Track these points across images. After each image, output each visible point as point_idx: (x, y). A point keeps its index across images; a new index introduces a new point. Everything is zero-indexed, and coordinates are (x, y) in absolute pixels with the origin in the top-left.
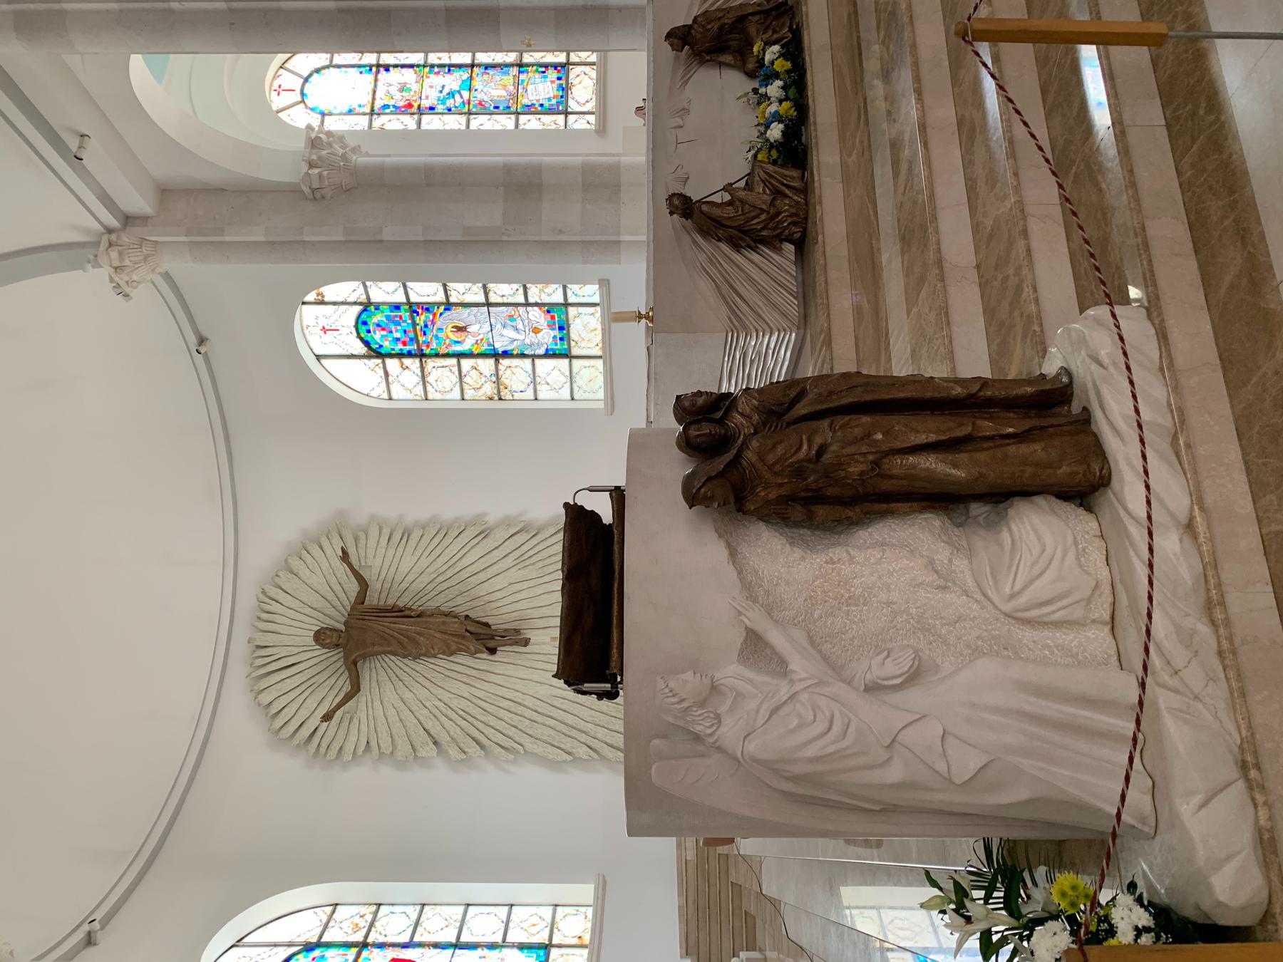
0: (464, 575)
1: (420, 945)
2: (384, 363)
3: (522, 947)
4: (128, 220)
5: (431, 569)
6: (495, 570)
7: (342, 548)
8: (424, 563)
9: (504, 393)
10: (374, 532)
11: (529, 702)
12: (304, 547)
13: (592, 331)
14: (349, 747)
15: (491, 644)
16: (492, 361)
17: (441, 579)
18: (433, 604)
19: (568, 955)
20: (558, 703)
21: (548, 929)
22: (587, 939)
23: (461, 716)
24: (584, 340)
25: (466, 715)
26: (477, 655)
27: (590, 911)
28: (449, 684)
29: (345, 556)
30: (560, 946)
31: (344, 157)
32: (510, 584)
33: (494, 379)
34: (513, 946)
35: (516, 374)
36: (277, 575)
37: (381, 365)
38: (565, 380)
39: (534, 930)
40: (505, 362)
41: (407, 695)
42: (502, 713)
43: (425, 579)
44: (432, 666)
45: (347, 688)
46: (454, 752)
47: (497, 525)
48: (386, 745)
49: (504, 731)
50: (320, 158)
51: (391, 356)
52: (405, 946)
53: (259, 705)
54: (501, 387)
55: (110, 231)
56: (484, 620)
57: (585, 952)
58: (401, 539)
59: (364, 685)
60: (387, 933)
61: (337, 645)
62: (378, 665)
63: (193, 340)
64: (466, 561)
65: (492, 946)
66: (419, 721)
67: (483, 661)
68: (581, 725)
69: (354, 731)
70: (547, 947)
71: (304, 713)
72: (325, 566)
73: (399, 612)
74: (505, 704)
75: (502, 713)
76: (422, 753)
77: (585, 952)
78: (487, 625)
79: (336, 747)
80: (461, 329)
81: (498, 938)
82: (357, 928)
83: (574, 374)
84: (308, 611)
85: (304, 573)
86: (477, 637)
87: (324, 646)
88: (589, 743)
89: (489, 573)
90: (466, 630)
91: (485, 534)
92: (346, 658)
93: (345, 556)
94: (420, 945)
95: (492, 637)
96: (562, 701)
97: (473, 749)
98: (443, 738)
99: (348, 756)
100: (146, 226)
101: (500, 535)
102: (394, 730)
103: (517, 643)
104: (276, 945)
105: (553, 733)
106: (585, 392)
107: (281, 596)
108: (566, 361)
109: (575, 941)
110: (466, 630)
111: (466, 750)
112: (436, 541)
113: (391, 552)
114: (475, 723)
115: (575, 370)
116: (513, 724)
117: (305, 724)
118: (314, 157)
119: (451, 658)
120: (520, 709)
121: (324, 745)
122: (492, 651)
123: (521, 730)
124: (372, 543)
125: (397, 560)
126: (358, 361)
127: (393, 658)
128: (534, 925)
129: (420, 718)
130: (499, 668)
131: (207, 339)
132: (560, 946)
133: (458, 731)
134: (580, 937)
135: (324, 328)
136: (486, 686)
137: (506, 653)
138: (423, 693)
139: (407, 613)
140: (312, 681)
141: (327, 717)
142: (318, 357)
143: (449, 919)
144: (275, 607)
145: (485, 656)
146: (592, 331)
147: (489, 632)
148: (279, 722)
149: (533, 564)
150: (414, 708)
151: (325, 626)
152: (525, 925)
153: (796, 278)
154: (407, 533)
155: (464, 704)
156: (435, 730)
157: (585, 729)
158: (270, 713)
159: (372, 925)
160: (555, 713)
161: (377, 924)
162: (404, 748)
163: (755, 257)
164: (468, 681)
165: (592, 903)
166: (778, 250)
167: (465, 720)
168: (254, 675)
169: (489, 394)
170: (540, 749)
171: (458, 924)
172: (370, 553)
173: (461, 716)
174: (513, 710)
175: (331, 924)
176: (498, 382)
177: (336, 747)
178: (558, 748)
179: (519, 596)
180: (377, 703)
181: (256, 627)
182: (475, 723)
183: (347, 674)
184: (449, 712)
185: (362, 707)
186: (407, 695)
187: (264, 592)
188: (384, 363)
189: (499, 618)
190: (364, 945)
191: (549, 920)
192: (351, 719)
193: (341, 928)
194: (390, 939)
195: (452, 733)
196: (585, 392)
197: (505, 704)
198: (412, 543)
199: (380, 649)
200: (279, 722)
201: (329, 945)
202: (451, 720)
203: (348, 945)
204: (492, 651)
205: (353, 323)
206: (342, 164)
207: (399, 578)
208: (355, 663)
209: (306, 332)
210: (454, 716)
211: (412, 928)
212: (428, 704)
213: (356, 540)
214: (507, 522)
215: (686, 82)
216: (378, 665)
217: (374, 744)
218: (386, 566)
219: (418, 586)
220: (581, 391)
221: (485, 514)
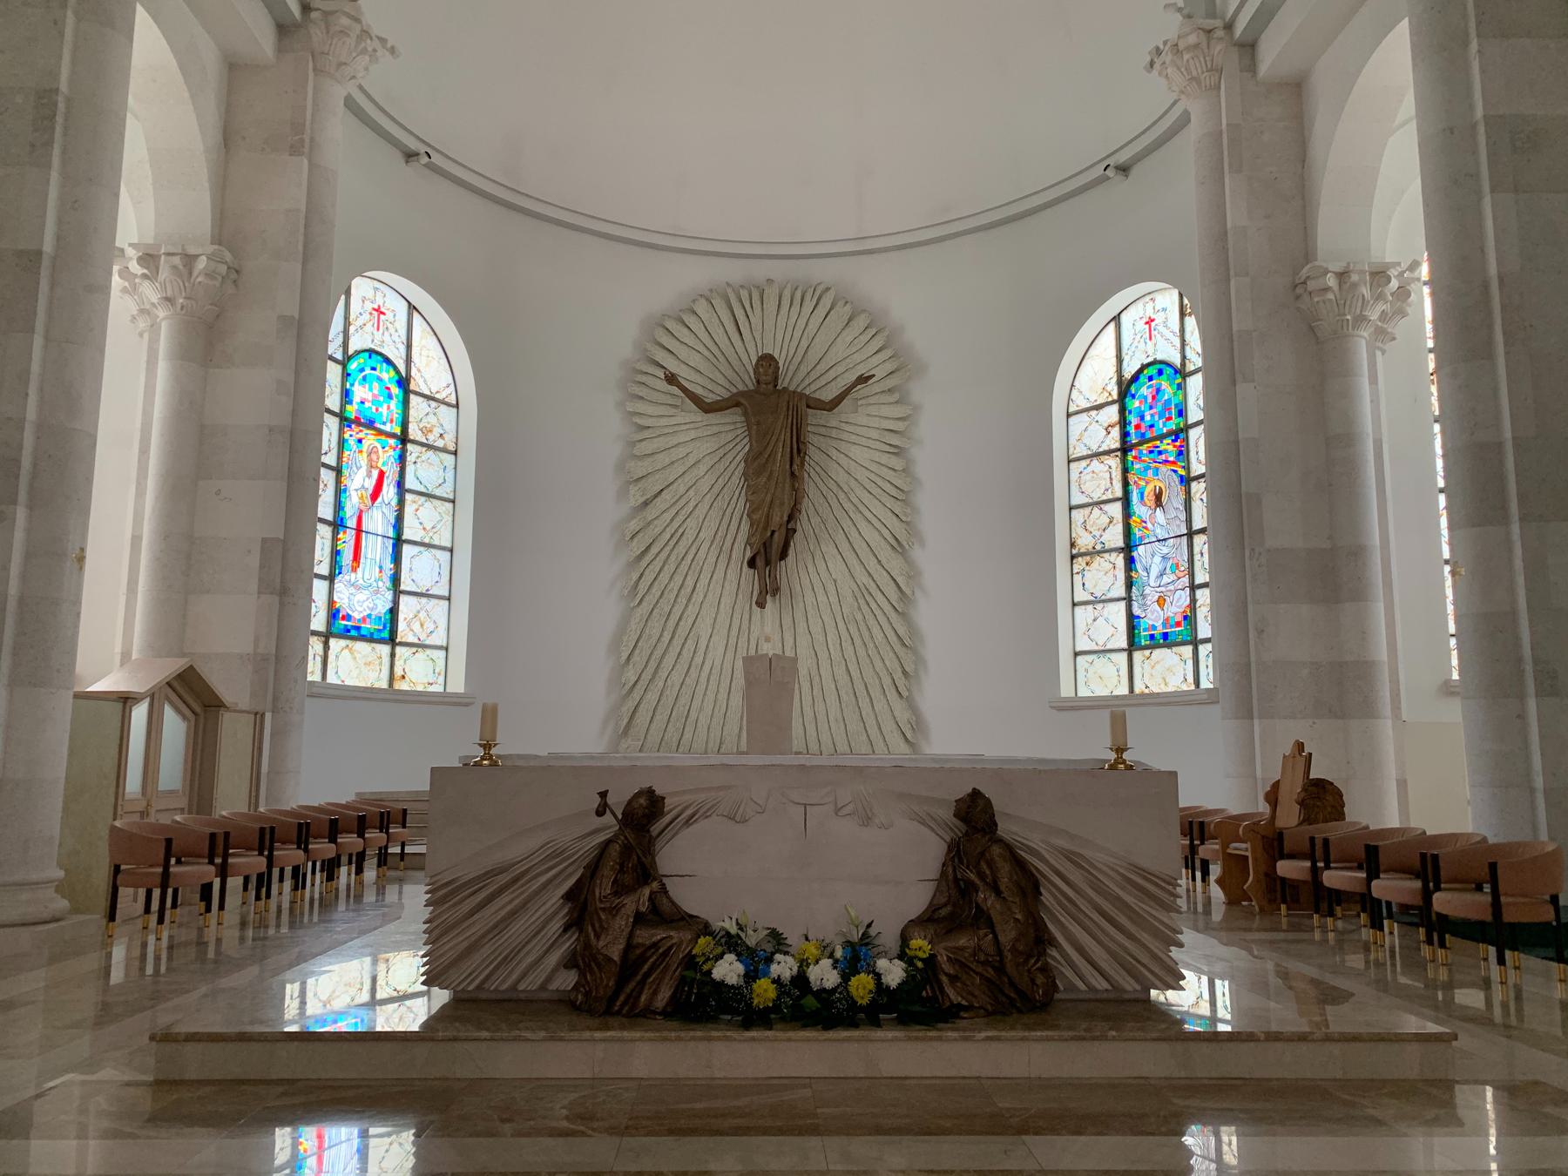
0: (846, 524)
1: (401, 503)
2: (1113, 402)
3: (394, 611)
4: (1249, 47)
5: (853, 483)
6: (852, 561)
7: (874, 376)
8: (861, 474)
9: (1081, 561)
11: (692, 610)
12: (878, 327)
13: (1164, 679)
14: (640, 407)
15: (760, 562)
16: (1121, 544)
17: (842, 496)
18: (810, 489)
19: (381, 664)
20: (690, 644)
21: (416, 641)
23: (676, 531)
24: (1153, 667)
26: (748, 547)
27: (438, 688)
30: (393, 655)
31: (1361, 319)
32: (835, 581)
33: (1098, 547)
34: (396, 602)
35: (1105, 576)
36: (847, 302)
37: (1110, 399)
38: (1101, 643)
39: (416, 626)
40: (1120, 560)
41: (703, 468)
42: (678, 579)
43: (841, 477)
44: (737, 493)
45: (710, 398)
46: (634, 525)
47: (908, 561)
49: (656, 583)
50: (1355, 286)
51: (1123, 411)
52: (400, 485)
53: (694, 301)
54: (1088, 558)
55: (1229, 27)
56: (791, 552)
57: (384, 685)
58: (890, 445)
59: (714, 418)
60: (418, 465)
61: (758, 382)
62: (739, 432)
63: (1122, 158)
64: (862, 525)
65: (396, 580)
66: (672, 483)
67: (741, 552)
68: (663, 674)
70: (392, 640)
71: (682, 352)
72: (858, 357)
73: (798, 449)
74: (690, 582)
75: (678, 579)
76: (633, 489)
77: (384, 685)
78: (783, 555)
79: (642, 392)
80: (1158, 497)
82: (426, 431)
83: (1108, 655)
84: (804, 344)
85: (848, 336)
86: (766, 545)
88: (641, 682)
89: (848, 554)
90: (773, 532)
91: (898, 547)
92: (742, 394)
93: (863, 379)
94: (401, 503)
95: (768, 563)
96: (693, 649)
97: (637, 547)
98: (651, 513)
100: (1241, 71)
101: (895, 564)
102: (660, 456)
103: (763, 593)
104: (409, 347)
105: (654, 640)
106: (1086, 671)
107: (821, 312)
108: (1124, 645)
109: (398, 671)
110: (773, 532)
111: (636, 540)
112: (888, 487)
113: (874, 434)
114: (668, 548)
115: (1113, 656)
116: (666, 592)
117: (671, 355)
118: (1355, 278)
119: (745, 516)
120: (683, 600)
121: (643, 378)
122: (752, 563)
123: (658, 602)
125: (864, 441)
126: (1115, 369)
127: (747, 448)
128: (422, 625)
129: (676, 484)
130: (732, 575)
131: (1127, 176)
132: (393, 655)
133: (658, 530)
134: (403, 677)
135: (1152, 320)
137: (751, 580)
138: (704, 486)
139: (797, 461)
140: (722, 359)
141: (671, 379)
142: (1117, 319)
143: (434, 530)
145: (749, 554)
146: (1164, 679)
147: (773, 561)
149: (860, 608)
150: (687, 478)
151: (781, 365)
152: (422, 615)
153: (514, 988)
154: (898, 452)
155: (690, 535)
156: (660, 504)
157: (657, 678)
158: (683, 314)
159: (429, 447)
160: (677, 642)
161: (431, 453)
162: (640, 468)
163: (556, 926)
164: (718, 537)
165: (448, 690)
166: (570, 962)
167: (672, 536)
168: (729, 291)
169: (1079, 542)
170: (634, 626)
171: (427, 540)
172: (873, 410)
173: (676, 531)
174: (682, 591)
175: (433, 404)
176: (1093, 553)
177: (642, 392)
178: (635, 646)
179: (820, 592)
180: (693, 434)
181: (796, 289)
182: (668, 548)
183: (726, 395)
184: (681, 518)
185: (692, 418)
186: (703, 468)
187: (828, 289)
188: (1113, 402)
189: (789, 569)
190: (404, 439)
191: (427, 642)
192: (676, 406)
193: (427, 414)
194: (410, 469)
195: (656, 522)
196: (1086, 671)
197: (690, 582)
198: (884, 459)
199: (754, 432)
200: (671, 325)
201: (406, 403)
202: (672, 520)
203: (405, 425)
204: (752, 563)
205: (1159, 357)
206: (1349, 317)
207: (843, 446)
208: (737, 405)
209: (1147, 298)
210: (676, 524)
211: (424, 490)
212: (691, 492)
214: (913, 574)
215: (923, 823)
216: (739, 432)
217: (646, 434)
218: (858, 430)
220: (1087, 665)
221: (922, 544)
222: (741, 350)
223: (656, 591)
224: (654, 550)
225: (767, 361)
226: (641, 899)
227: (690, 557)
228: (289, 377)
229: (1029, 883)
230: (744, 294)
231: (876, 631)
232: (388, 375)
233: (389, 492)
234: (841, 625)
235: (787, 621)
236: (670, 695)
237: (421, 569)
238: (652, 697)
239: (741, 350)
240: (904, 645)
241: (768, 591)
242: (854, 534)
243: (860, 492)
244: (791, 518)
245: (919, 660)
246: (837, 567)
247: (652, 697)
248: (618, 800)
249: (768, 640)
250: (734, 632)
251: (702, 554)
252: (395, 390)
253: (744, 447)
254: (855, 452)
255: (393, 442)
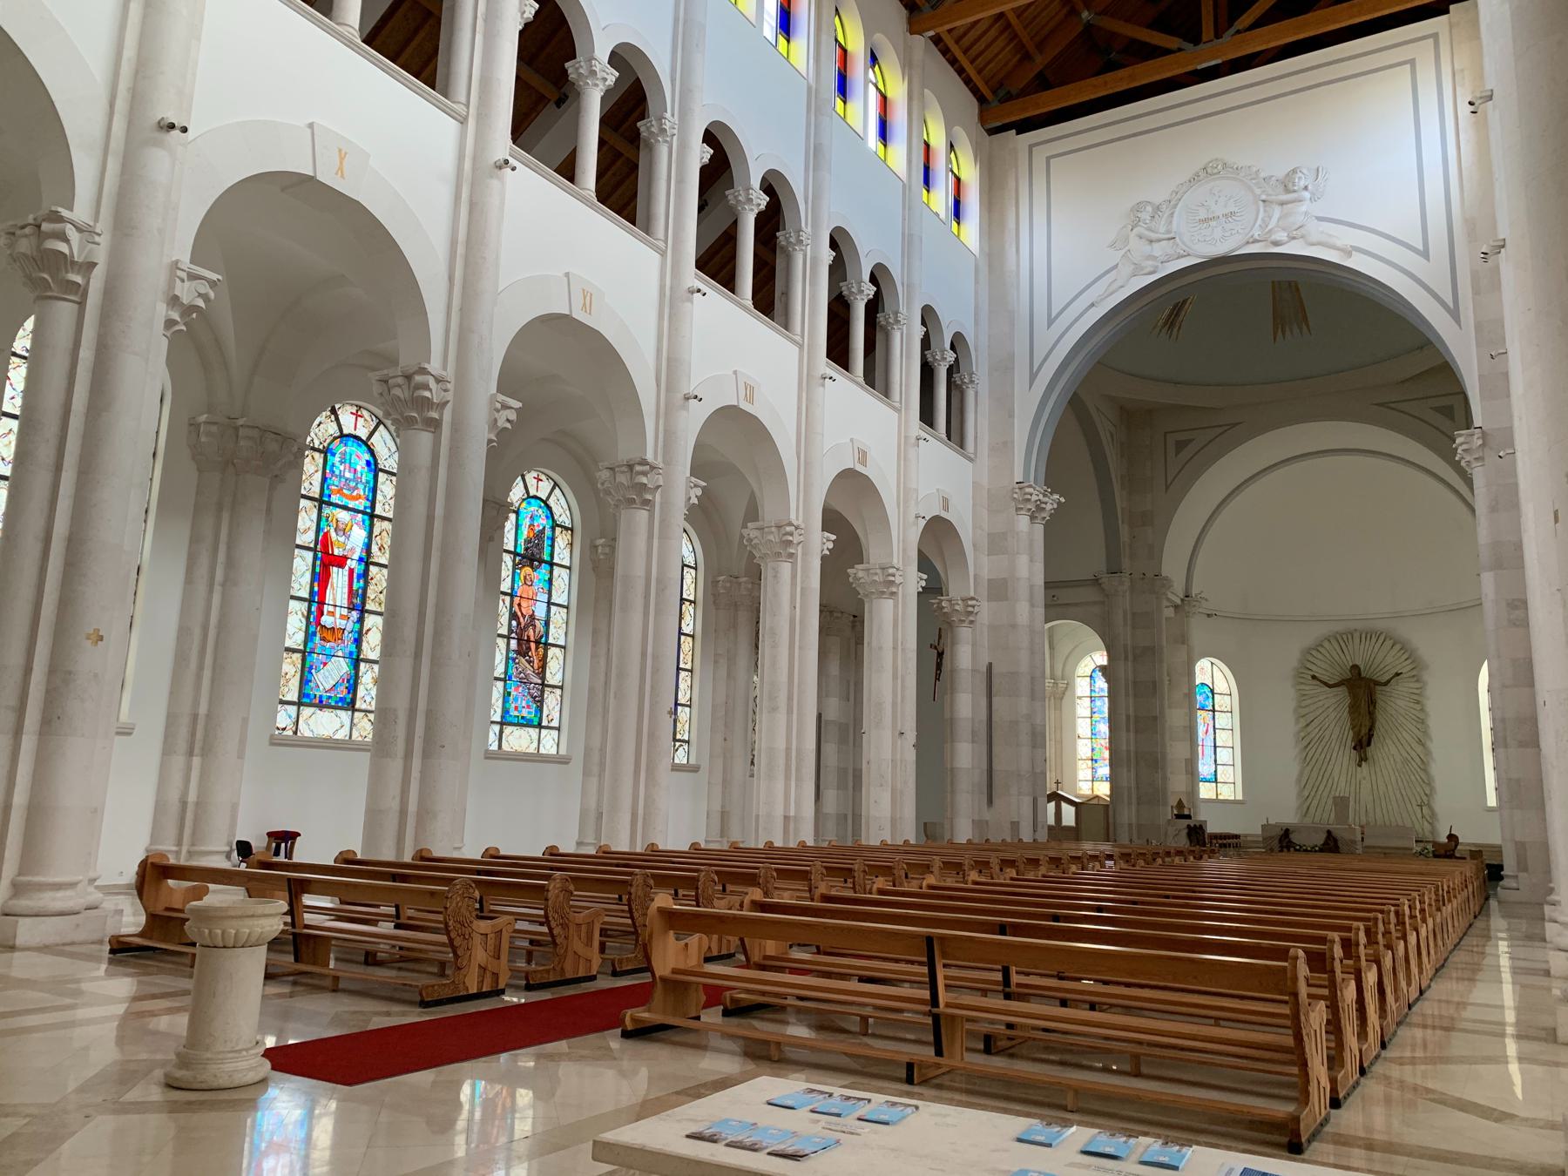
1: (1215, 733)
8: (1402, 712)
10: (1418, 685)
11: (1330, 767)
14: (1303, 687)
15: (1358, 747)
22: (1220, 797)
25: (1321, 739)
28: (1338, 729)
29: (1398, 674)
42: (1323, 756)
46: (1302, 734)
48: (1304, 704)
53: (1322, 641)
57: (1215, 797)
65: (1215, 761)
67: (1350, 744)
68: (1320, 792)
69: (1311, 687)
71: (1319, 663)
72: (1397, 662)
73: (1372, 702)
74: (1328, 757)
75: (1323, 756)
76: (1302, 720)
77: (1215, 797)
78: (1369, 744)
79: (1302, 680)
81: (1218, 762)
84: (1373, 656)
86: (1360, 742)
87: (1350, 671)
89: (1398, 744)
91: (1420, 742)
92: (1343, 680)
93: (1398, 674)
94: (1215, 733)
95: (1361, 748)
97: (1305, 743)
98: (1309, 729)
99: (1298, 687)
101: (1419, 749)
103: (1361, 760)
107: (1380, 641)
109: (1219, 792)
112: (1413, 717)
120: (1325, 764)
121: (1302, 675)
122: (1355, 748)
124: (1412, 685)
130: (1347, 751)
136: (1337, 747)
138: (1333, 715)
141: (1314, 677)
144: (1374, 640)
145: (1353, 744)
148: (1314, 652)
151: (1362, 669)
155: (1327, 738)
158: (1318, 646)
162: (1304, 711)
168: (1338, 636)
177: (1302, 680)
187: (1381, 633)
189: (1371, 751)
190: (1214, 711)
197: (1328, 757)
198: (1412, 705)
203: (1213, 706)
208: (1343, 684)
213: (1414, 676)
214: (1428, 753)
219: (1388, 708)
221: (1431, 740)
222: (1345, 660)
223: (1314, 760)
224: (1312, 744)
225: (1355, 667)
226: (1287, 840)
227: (1327, 747)
228: (1188, 711)
229: (1335, 841)
230: (1344, 637)
231: (1413, 777)
232: (1206, 690)
233: (1211, 730)
234: (1397, 774)
235: (1373, 772)
236: (1323, 801)
237: (1224, 756)
238: (1315, 802)
239: (1345, 660)
240: (1424, 782)
241: (1363, 759)
242: (1399, 736)
243: (1401, 718)
244: (1370, 730)
245: (1432, 789)
246: (1393, 750)
247: (1315, 802)
248: (1284, 829)
249: (1364, 778)
250: (1350, 774)
251: (1333, 745)
252: (1210, 695)
253: (1348, 701)
254: (1398, 702)
255: (1211, 713)
